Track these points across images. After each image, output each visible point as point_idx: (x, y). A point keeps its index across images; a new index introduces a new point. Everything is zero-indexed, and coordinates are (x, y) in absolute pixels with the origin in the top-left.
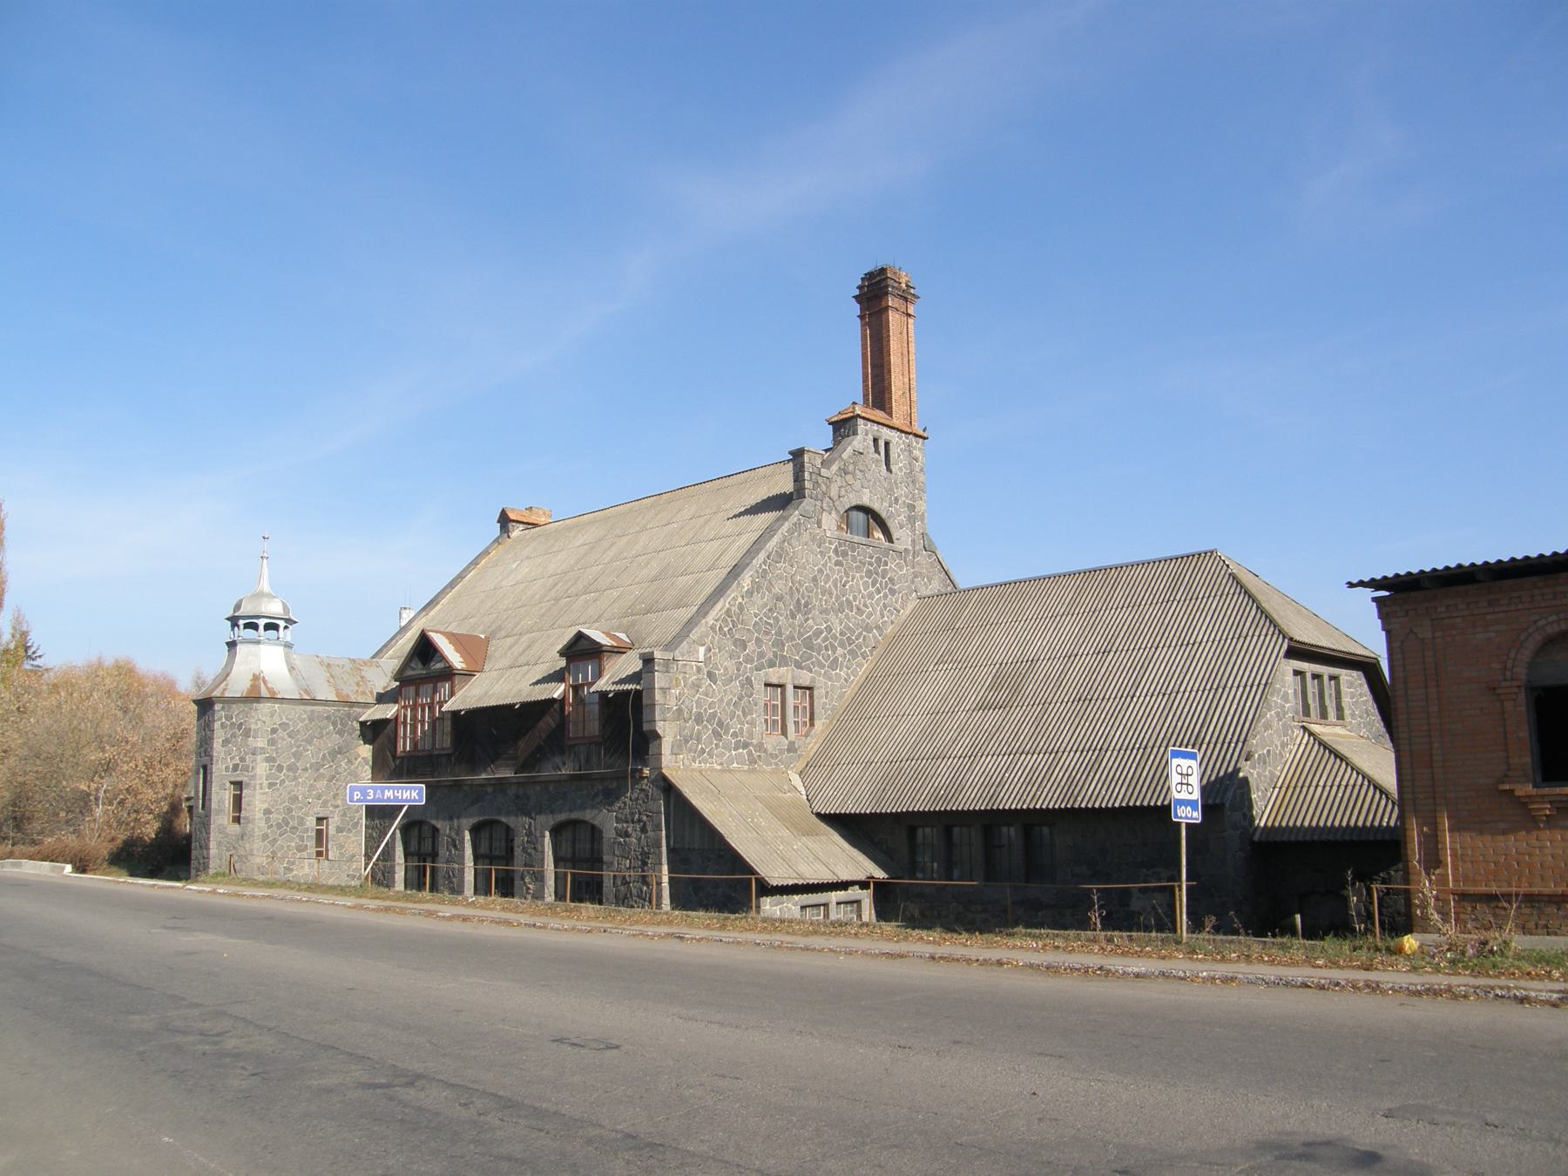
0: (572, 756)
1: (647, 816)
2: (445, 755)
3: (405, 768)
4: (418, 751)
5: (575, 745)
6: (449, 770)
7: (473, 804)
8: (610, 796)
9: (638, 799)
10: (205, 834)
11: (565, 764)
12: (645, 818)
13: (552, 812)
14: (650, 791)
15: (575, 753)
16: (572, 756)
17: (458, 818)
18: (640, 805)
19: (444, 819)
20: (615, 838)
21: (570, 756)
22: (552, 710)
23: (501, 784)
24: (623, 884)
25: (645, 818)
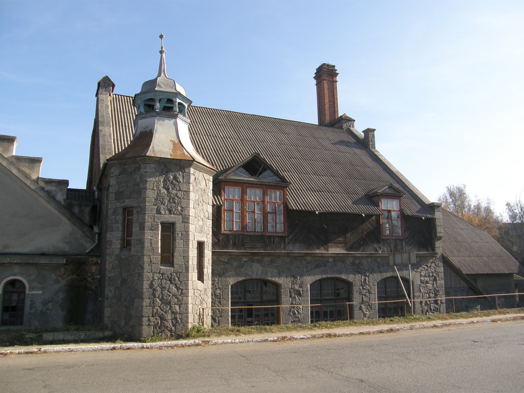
0: (386, 244)
1: (436, 274)
2: (278, 236)
3: (231, 242)
4: (247, 231)
5: (388, 239)
6: (282, 247)
7: (315, 268)
8: (415, 266)
9: (431, 266)
10: (174, 289)
11: (380, 248)
12: (435, 275)
13: (380, 272)
14: (437, 263)
15: (387, 244)
16: (386, 244)
17: (301, 276)
18: (432, 269)
19: (287, 277)
20: (420, 285)
21: (384, 244)
22: (370, 220)
23: (337, 258)
24: (425, 305)
25: (435, 275)
